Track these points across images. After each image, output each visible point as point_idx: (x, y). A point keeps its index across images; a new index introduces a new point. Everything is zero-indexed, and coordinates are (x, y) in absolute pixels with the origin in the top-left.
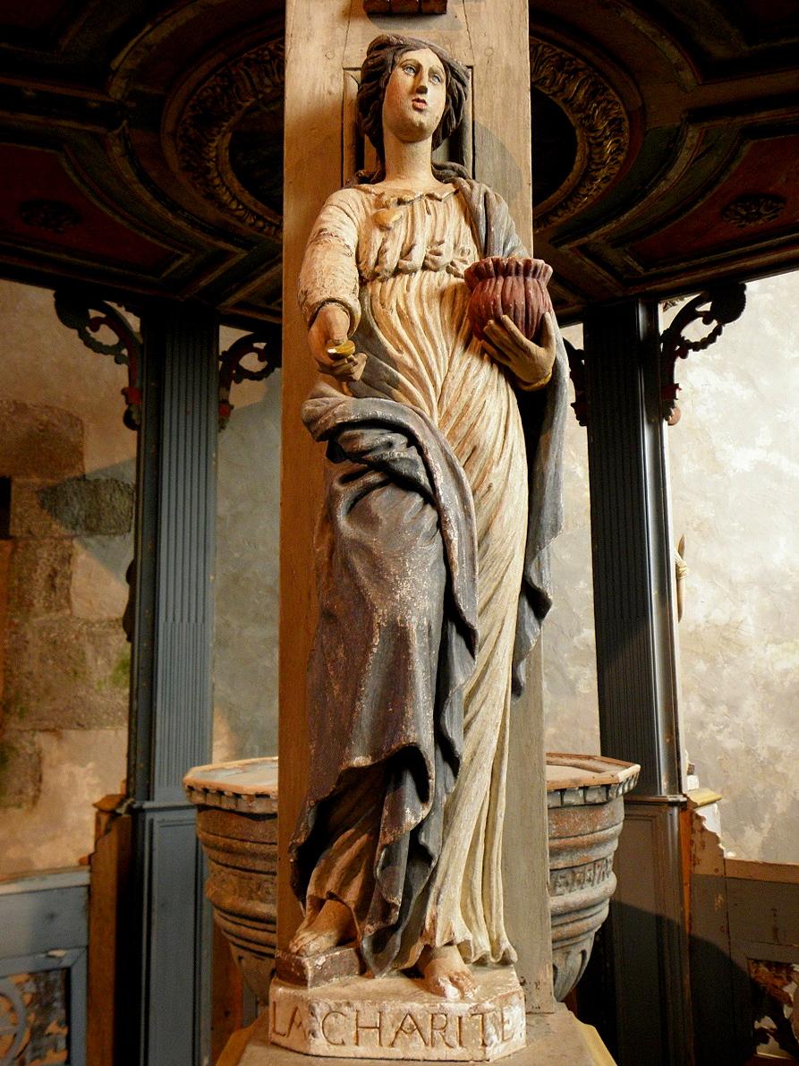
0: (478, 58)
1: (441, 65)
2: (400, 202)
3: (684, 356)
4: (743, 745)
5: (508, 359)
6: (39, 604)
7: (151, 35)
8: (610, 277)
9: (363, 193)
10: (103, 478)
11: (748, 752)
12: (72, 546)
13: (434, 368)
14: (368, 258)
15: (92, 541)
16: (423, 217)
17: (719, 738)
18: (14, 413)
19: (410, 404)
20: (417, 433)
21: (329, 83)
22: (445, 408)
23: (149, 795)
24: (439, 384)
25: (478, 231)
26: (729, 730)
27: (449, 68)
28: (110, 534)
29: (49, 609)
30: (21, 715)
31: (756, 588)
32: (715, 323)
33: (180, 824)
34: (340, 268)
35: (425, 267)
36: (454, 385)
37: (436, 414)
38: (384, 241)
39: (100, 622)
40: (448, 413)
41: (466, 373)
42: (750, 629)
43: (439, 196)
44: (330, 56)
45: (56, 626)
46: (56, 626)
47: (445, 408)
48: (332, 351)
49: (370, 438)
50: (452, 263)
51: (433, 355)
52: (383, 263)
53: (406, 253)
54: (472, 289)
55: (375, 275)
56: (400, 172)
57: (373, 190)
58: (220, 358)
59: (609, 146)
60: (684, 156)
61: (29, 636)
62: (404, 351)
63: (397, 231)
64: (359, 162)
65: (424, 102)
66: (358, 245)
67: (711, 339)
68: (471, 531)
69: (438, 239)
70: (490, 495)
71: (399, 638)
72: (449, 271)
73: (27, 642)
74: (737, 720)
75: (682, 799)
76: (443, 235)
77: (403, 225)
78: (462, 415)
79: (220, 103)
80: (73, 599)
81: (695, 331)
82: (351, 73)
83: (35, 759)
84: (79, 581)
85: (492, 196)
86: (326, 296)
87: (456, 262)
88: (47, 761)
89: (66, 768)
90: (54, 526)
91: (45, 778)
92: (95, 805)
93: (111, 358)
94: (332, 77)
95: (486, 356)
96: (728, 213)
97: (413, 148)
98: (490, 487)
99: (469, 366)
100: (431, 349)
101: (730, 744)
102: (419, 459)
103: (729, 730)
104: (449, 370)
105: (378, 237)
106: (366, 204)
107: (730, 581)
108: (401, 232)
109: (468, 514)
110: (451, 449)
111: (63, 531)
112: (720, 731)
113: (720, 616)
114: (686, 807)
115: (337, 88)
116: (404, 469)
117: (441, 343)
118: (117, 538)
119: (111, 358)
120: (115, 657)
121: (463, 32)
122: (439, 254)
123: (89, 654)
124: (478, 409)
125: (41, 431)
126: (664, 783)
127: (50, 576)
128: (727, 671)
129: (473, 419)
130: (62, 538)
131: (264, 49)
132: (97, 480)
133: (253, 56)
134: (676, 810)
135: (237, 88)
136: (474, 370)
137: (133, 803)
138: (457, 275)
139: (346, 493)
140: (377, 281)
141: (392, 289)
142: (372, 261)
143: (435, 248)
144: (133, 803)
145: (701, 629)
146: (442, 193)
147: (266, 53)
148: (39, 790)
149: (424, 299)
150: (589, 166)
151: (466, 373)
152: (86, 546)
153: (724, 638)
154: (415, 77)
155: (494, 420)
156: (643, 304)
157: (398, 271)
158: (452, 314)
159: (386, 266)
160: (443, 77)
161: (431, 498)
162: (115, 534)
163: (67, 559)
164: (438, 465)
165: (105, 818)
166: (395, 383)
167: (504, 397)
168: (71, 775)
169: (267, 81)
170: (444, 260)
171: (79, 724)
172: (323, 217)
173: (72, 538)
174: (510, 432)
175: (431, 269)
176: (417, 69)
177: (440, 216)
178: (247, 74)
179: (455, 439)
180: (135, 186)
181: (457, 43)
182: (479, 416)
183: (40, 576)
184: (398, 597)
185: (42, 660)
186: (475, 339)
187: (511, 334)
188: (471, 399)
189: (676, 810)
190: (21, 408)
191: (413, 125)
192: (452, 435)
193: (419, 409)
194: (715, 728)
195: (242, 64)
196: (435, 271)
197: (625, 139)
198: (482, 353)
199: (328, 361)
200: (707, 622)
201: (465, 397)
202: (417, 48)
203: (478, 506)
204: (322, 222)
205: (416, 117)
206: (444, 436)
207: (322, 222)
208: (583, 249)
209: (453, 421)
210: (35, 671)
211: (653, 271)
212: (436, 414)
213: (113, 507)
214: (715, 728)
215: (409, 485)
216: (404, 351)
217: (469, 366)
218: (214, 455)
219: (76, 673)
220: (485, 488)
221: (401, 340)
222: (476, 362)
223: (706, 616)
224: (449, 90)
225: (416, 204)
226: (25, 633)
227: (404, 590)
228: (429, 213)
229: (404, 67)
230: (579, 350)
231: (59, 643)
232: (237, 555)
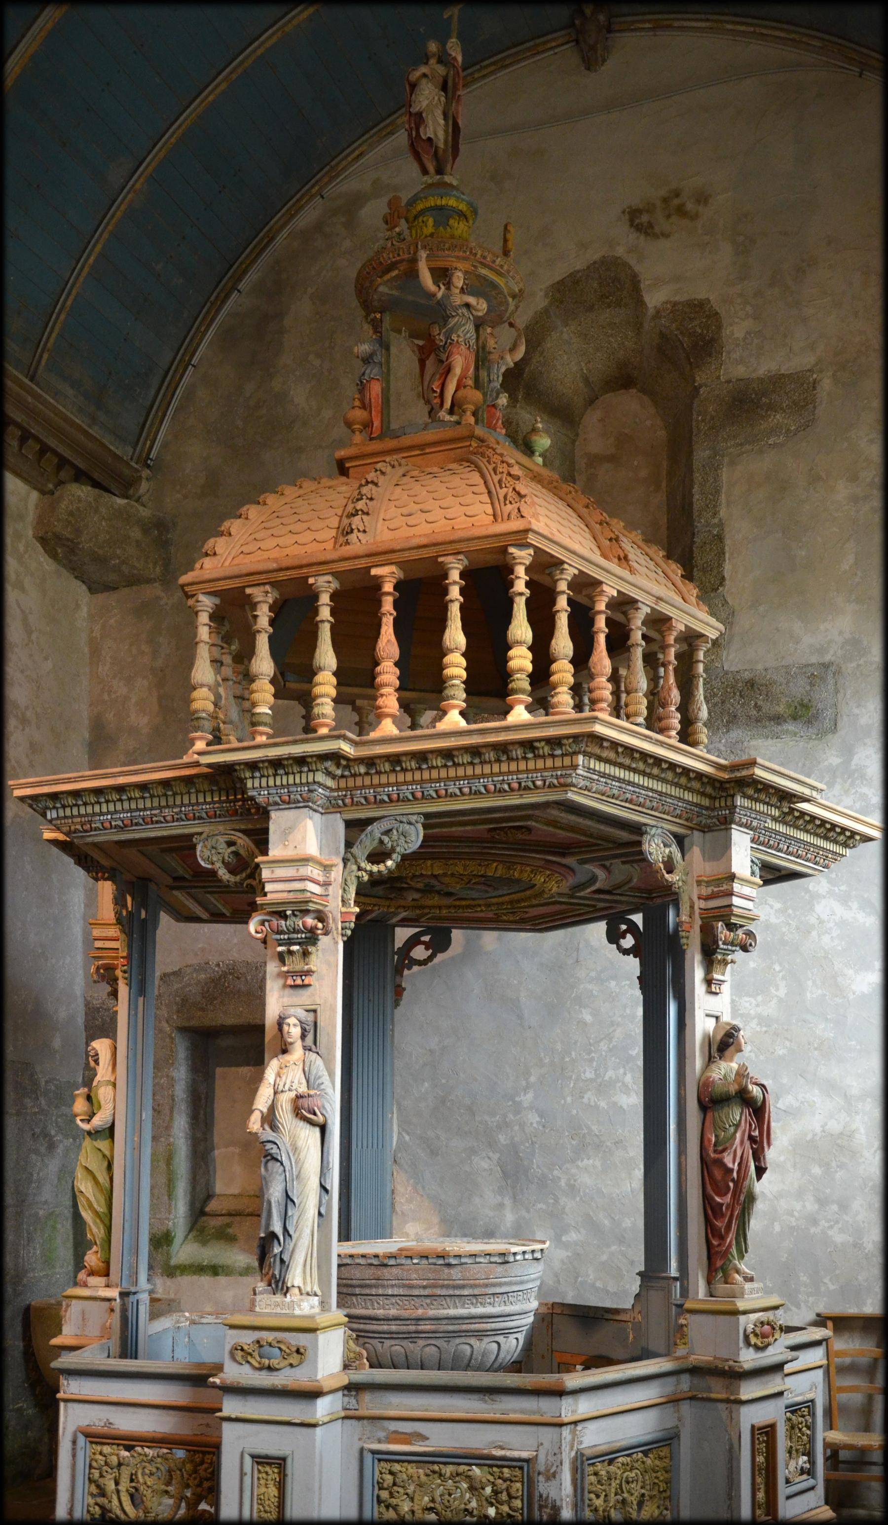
4: (851, 1240)
11: (855, 1245)
17: (830, 1233)
26: (840, 1226)
31: (869, 1100)
49: (269, 1146)
74: (846, 1218)
101: (839, 1238)
103: (840, 1226)
107: (846, 1095)
112: (831, 1227)
113: (835, 1126)
116: (275, 1156)
128: (840, 1175)
139: (263, 1160)
145: (818, 1138)
153: (838, 1145)
161: (282, 1164)
194: (826, 1225)
200: (823, 1131)
214: (826, 1225)
215: (277, 1160)
223: (822, 1127)
227: (271, 1190)
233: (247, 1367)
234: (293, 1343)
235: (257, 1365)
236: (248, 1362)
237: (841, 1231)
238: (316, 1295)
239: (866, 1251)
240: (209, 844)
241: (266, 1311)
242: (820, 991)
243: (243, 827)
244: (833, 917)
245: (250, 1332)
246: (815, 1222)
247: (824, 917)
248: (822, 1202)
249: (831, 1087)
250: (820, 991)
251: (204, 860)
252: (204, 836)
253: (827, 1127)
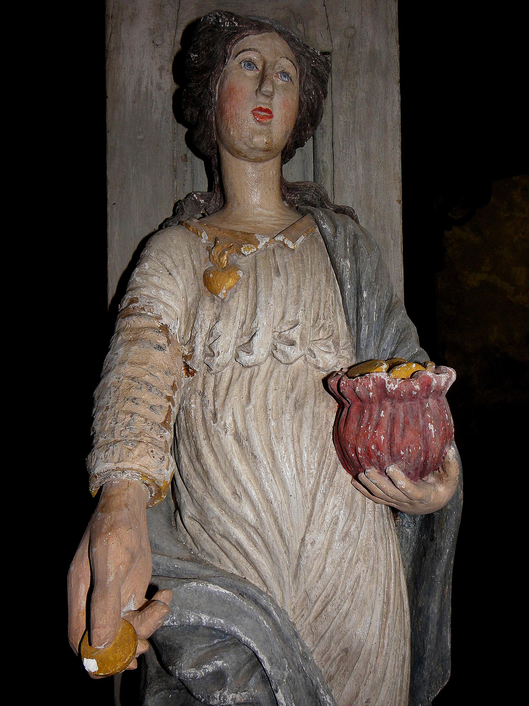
0: (337, 41)
21: (158, 76)
22: (302, 587)
34: (147, 378)
43: (291, 245)
44: (159, 42)
62: (244, 499)
63: (233, 304)
94: (161, 69)
181: (311, 23)
216: (244, 499)
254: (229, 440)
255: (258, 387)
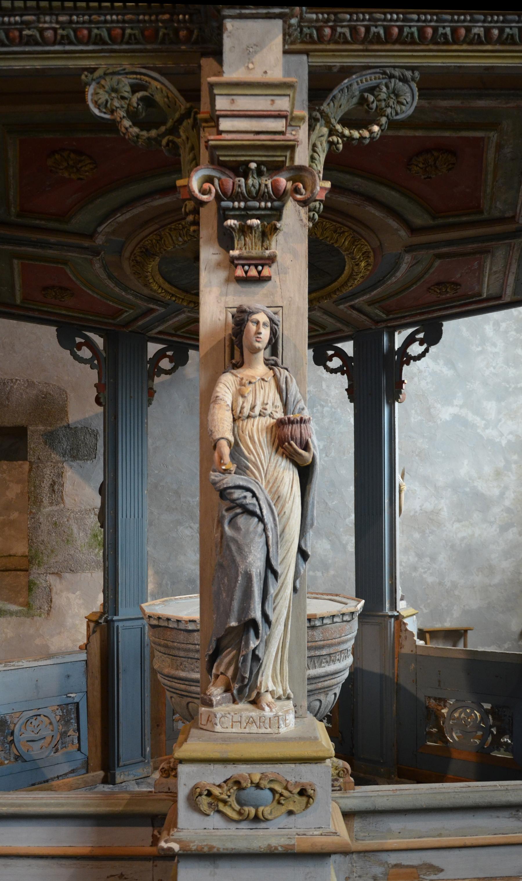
1: (268, 320)
2: (250, 383)
3: (408, 364)
4: (437, 580)
5: (293, 457)
6: (46, 501)
7: (120, 218)
8: (368, 319)
9: (234, 377)
10: (80, 426)
11: (440, 584)
12: (63, 467)
13: (263, 462)
14: (237, 410)
15: (74, 464)
16: (260, 391)
17: (425, 576)
18: (27, 388)
19: (254, 478)
20: (256, 492)
22: (267, 479)
23: (116, 613)
24: (265, 468)
25: (282, 397)
26: (431, 571)
27: (271, 320)
28: (84, 460)
29: (51, 504)
30: (39, 565)
31: (449, 490)
32: (425, 346)
33: (132, 628)
35: (260, 415)
36: (271, 469)
37: (264, 481)
38: (243, 403)
39: (81, 511)
40: (269, 482)
41: (276, 464)
42: (445, 514)
45: (56, 514)
46: (56, 514)
47: (267, 479)
48: (224, 467)
49: (237, 494)
50: (271, 413)
51: (263, 457)
52: (242, 414)
53: (253, 408)
54: (279, 427)
55: (239, 417)
56: (251, 366)
57: (239, 376)
58: (148, 362)
59: (363, 264)
60: (404, 267)
61: (41, 520)
64: (232, 357)
65: (260, 338)
66: (232, 402)
67: (423, 355)
68: (277, 532)
69: (265, 402)
70: (284, 516)
71: (248, 578)
72: (270, 416)
73: (41, 523)
75: (396, 614)
76: (267, 400)
77: (251, 395)
78: (274, 483)
79: (155, 247)
80: (65, 498)
81: (415, 349)
82: (229, 309)
83: (48, 589)
84: (68, 487)
85: (289, 379)
86: (220, 436)
87: (273, 412)
88: (54, 590)
89: (64, 594)
90: (53, 455)
91: (53, 600)
92: (86, 618)
93: (88, 366)
94: (220, 312)
95: (284, 455)
96: (430, 291)
97: (256, 355)
98: (285, 513)
99: (277, 461)
100: (262, 454)
101: (430, 579)
102: (256, 503)
103: (431, 571)
104: (269, 463)
105: (241, 400)
106: (236, 383)
107: (435, 486)
108: (250, 398)
109: (276, 525)
110: (269, 498)
111: (58, 458)
112: (425, 572)
113: (429, 506)
114: (398, 618)
115: (222, 317)
116: (251, 508)
117: (266, 451)
118: (89, 462)
119: (88, 366)
120: (89, 532)
121: (278, 290)
122: (266, 409)
123: (75, 531)
124: (281, 480)
125: (43, 398)
126: (387, 605)
127: (51, 484)
128: (431, 538)
129: (279, 484)
130: (57, 462)
131: (179, 224)
132: (76, 428)
133: (173, 227)
134: (393, 620)
135: (164, 241)
136: (279, 462)
137: (108, 617)
138: (273, 418)
139: (228, 516)
140: (240, 420)
141: (246, 425)
142: (238, 412)
143: (264, 406)
144: (108, 617)
145: (417, 514)
146: (268, 378)
147: (180, 226)
148: (51, 607)
149: (260, 430)
150: (352, 273)
151: (276, 464)
152: (71, 467)
153: (430, 519)
154: (257, 326)
155: (287, 483)
156: (387, 332)
157: (249, 417)
158: (271, 437)
159: (244, 415)
160: (269, 324)
161: (261, 519)
162: (87, 460)
163: (60, 475)
164: (264, 506)
165: (92, 625)
166: (248, 468)
167: (291, 473)
168: (68, 598)
169: (180, 239)
170: (268, 412)
171: (71, 570)
172: (218, 389)
173: (63, 462)
174: (294, 488)
175: (262, 416)
176: (258, 323)
177: (267, 392)
178: (170, 234)
179: (271, 493)
180: (106, 281)
182: (281, 483)
183: (46, 485)
184: (248, 561)
185: (49, 533)
186: (280, 448)
187: (295, 449)
188: (278, 475)
189: (393, 620)
190: (31, 384)
191: (256, 348)
192: (270, 491)
193: (257, 481)
194: (423, 571)
195: (167, 230)
196: (264, 417)
197: (371, 260)
198: (282, 455)
199: (222, 471)
200: (421, 510)
201: (275, 475)
202: (257, 313)
203: (280, 520)
204: (217, 392)
205: (257, 345)
206: (266, 492)
207: (217, 392)
208: (353, 307)
209: (271, 485)
210: (45, 540)
211: (391, 316)
212: (264, 481)
213: (86, 444)
214: (423, 571)
215: (253, 514)
217: (277, 461)
218: (146, 421)
219: (68, 541)
220: (283, 513)
221: (250, 449)
222: (280, 459)
223: (420, 506)
224: (271, 329)
225: (257, 383)
226: (39, 518)
227: (250, 559)
228: (262, 388)
229: (252, 322)
230: (351, 357)
231: (58, 523)
232: (156, 472)
233: (215, 820)
234: (292, 779)
235: (234, 816)
236: (219, 812)
237: (431, 574)
238: (288, 698)
239: (447, 587)
240: (107, 83)
241: (234, 730)
242: (419, 418)
243: (159, 64)
244: (428, 369)
245: (219, 767)
246: (415, 569)
247: (422, 368)
248: (420, 556)
249: (425, 481)
250: (419, 418)
251: (98, 107)
252: (97, 74)
253: (424, 507)
254: (247, 438)
255: (256, 423)
